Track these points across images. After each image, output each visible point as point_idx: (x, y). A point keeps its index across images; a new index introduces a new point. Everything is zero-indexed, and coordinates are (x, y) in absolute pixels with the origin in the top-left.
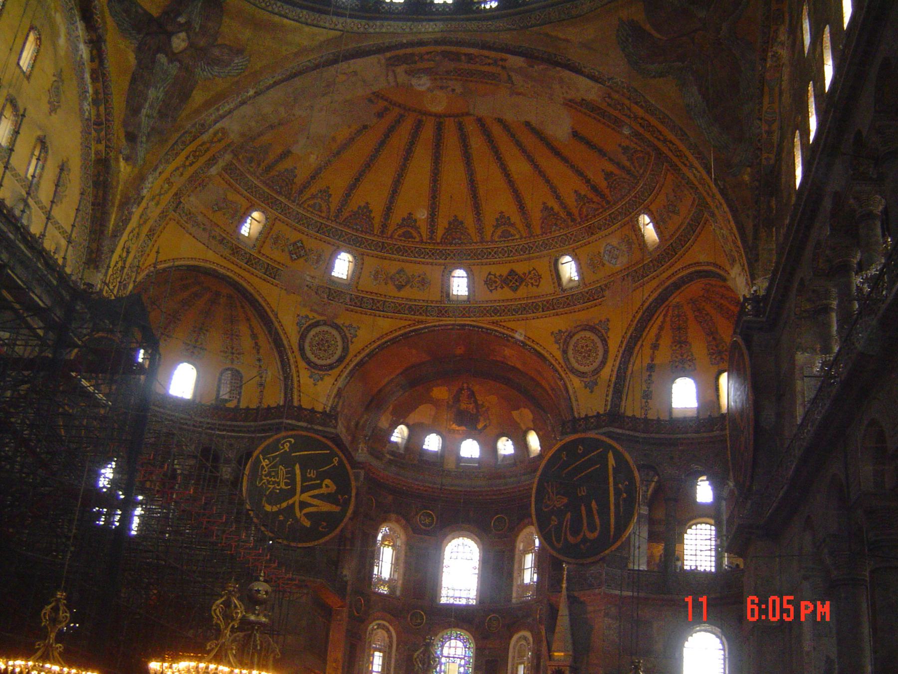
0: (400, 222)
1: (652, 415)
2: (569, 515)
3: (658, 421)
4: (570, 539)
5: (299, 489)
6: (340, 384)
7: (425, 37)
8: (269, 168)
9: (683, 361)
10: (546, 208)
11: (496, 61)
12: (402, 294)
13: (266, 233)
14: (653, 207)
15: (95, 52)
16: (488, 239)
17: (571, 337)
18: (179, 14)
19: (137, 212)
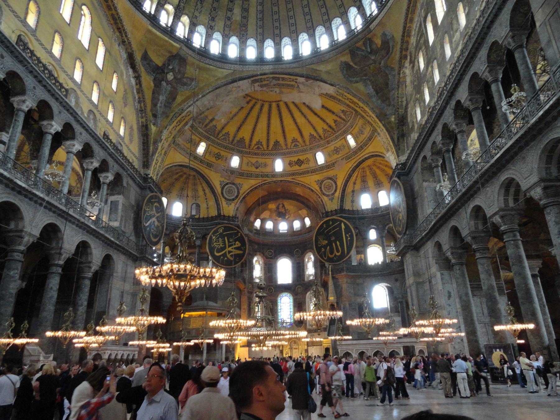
1: (354, 209)
2: (328, 248)
3: (358, 210)
4: (330, 255)
5: (227, 246)
6: (237, 206)
7: (267, 71)
9: (365, 188)
10: (311, 135)
11: (293, 80)
12: (258, 170)
13: (206, 151)
14: (353, 132)
15: (137, 81)
18: (169, 65)
19: (160, 145)
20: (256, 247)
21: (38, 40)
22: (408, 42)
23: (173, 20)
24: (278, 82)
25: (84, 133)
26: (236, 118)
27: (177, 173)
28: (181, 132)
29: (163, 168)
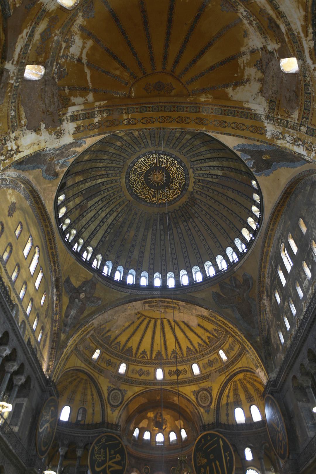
0: (141, 352)
5: (108, 459)
6: (120, 413)
8: (103, 335)
10: (188, 348)
11: (176, 303)
14: (224, 348)
16: (169, 358)
17: (199, 393)
19: (65, 350)
20: (133, 461)
21: (6, 270)
22: (263, 281)
23: (91, 257)
24: (164, 304)
25: (15, 339)
26: (127, 331)
27: (72, 377)
28: (83, 340)
29: (63, 371)
